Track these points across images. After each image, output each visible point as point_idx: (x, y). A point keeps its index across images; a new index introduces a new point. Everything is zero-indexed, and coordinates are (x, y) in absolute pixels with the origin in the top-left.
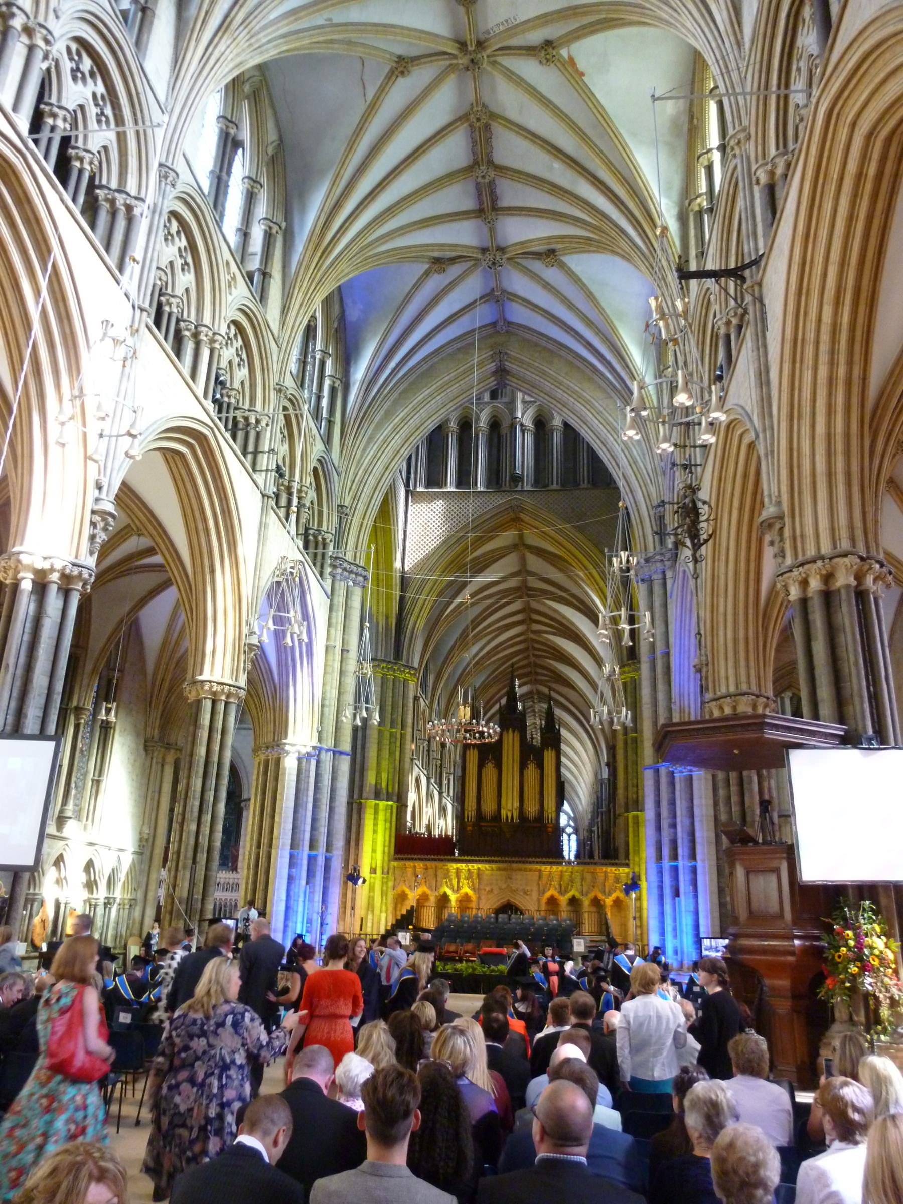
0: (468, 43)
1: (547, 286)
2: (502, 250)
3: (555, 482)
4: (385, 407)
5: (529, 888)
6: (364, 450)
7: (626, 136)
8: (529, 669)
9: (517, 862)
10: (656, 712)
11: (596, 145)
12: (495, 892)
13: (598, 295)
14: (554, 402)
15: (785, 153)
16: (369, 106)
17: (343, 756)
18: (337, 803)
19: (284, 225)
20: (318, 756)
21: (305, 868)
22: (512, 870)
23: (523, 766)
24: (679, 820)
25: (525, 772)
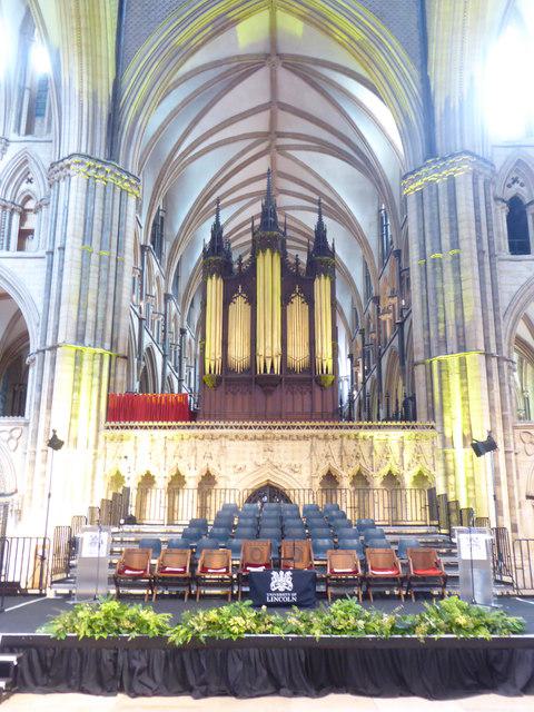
23: (286, 300)
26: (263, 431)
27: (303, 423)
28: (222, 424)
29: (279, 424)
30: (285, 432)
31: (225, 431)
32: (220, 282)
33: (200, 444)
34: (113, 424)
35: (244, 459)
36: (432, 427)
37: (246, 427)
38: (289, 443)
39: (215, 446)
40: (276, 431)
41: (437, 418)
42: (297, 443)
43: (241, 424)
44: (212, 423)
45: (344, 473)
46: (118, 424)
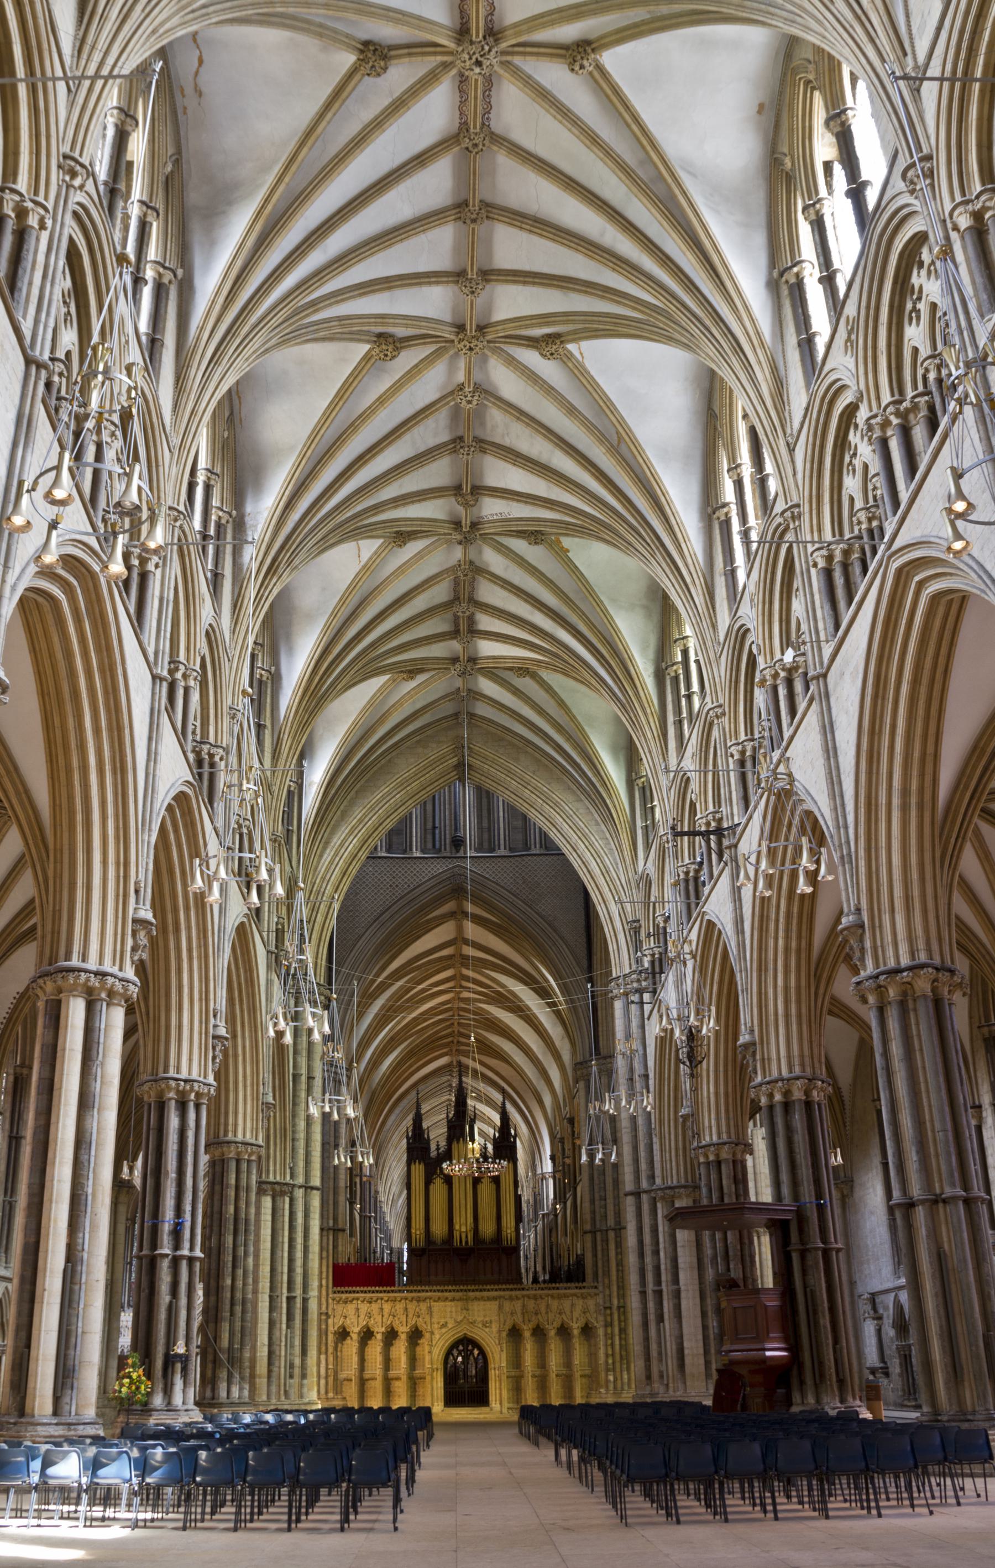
0: (463, 522)
1: (516, 692)
2: (473, 660)
3: (502, 847)
4: (342, 807)
5: (487, 1319)
6: (321, 856)
7: (606, 603)
8: (450, 1039)
9: (473, 1291)
10: (636, 1136)
11: (578, 607)
12: (450, 1326)
13: (569, 702)
14: (521, 801)
15: (752, 740)
16: (364, 567)
17: (315, 1192)
18: (311, 1242)
19: (273, 669)
20: (291, 1193)
21: (284, 1311)
22: (467, 1299)
24: (661, 1246)
25: (479, 1187)
26: (460, 1294)
27: (492, 1287)
28: (427, 1288)
29: (473, 1287)
30: (478, 1294)
31: (429, 1294)
32: (422, 1167)
33: (412, 1306)
34: (339, 1289)
35: (445, 1317)
36: (596, 1287)
37: (446, 1291)
38: (482, 1303)
39: (423, 1306)
40: (471, 1294)
41: (600, 1279)
42: (488, 1303)
43: (442, 1288)
44: (419, 1288)
45: (525, 1327)
46: (343, 1289)
